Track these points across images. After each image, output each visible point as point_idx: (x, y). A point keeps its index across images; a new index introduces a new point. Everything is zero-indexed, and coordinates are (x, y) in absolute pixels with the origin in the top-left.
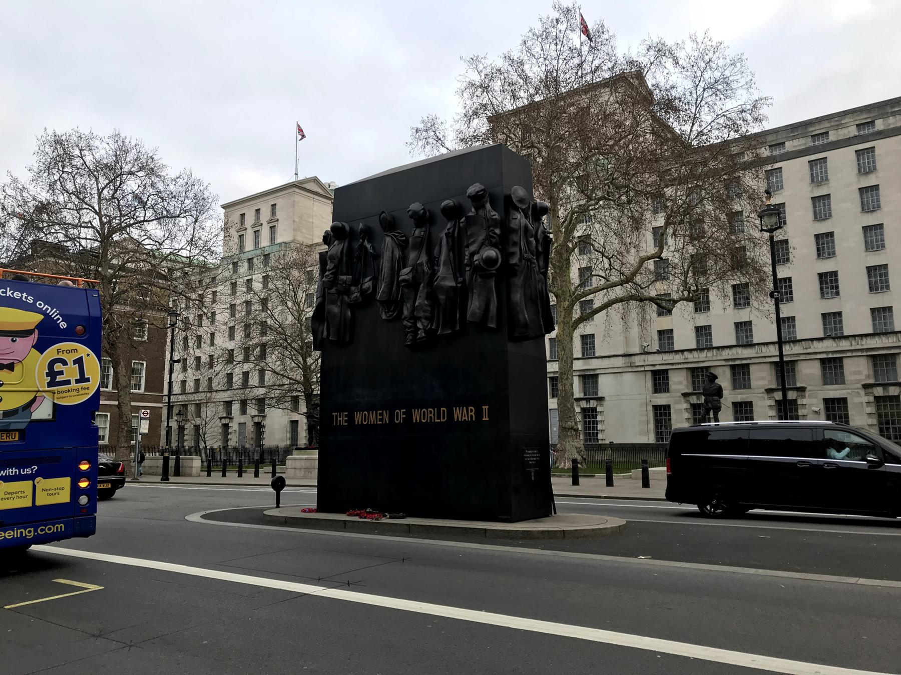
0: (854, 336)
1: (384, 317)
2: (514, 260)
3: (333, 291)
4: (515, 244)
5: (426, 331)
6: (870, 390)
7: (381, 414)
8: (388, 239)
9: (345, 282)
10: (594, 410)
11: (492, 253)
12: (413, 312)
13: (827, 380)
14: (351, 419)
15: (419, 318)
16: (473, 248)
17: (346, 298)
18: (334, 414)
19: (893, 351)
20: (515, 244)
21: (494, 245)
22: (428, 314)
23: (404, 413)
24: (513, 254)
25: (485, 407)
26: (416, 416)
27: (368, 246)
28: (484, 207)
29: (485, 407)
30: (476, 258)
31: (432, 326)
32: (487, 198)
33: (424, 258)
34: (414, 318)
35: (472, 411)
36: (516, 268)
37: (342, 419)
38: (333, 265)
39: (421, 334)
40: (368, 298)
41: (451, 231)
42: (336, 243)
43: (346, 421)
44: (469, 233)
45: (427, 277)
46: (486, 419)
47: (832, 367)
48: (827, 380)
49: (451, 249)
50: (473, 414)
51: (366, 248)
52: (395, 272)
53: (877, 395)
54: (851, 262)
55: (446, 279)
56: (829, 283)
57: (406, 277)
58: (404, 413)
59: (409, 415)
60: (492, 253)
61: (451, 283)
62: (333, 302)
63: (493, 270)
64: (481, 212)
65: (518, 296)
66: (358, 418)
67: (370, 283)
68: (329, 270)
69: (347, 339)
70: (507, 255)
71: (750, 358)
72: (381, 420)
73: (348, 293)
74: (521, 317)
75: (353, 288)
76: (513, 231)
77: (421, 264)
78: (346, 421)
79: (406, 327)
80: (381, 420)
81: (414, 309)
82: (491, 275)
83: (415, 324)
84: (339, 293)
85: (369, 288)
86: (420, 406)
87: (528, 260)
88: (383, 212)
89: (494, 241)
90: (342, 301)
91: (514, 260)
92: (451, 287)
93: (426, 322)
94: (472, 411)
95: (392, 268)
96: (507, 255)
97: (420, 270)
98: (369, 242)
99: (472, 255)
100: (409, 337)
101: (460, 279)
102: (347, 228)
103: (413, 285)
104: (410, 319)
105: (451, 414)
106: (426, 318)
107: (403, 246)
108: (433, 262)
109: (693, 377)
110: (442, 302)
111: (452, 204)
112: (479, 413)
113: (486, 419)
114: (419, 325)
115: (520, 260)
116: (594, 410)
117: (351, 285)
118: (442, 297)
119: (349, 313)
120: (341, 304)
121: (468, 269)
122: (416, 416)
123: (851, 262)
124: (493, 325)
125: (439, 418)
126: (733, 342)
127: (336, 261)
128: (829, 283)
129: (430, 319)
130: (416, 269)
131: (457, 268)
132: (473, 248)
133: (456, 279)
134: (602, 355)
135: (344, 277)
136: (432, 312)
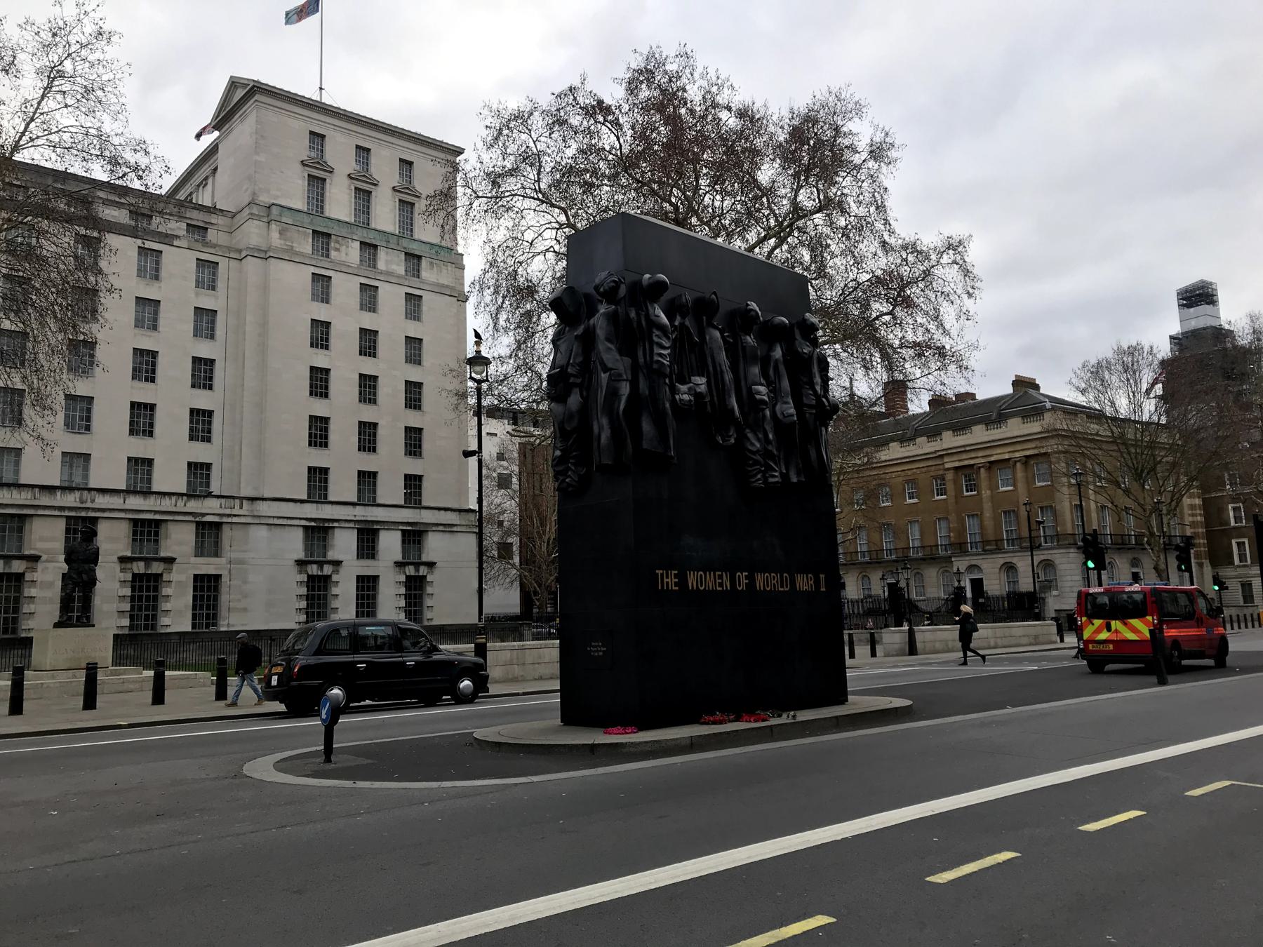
0: (33, 486)
6: (129, 566)
7: (721, 577)
10: (327, 578)
13: (200, 551)
18: (659, 572)
19: (157, 517)
26: (760, 580)
34: (767, 454)
46: (823, 589)
47: (368, 537)
48: (200, 551)
53: (136, 571)
54: (173, 395)
56: (142, 418)
59: (751, 579)
66: (692, 580)
71: (103, 510)
72: (721, 585)
79: (756, 462)
86: (763, 570)
105: (793, 582)
109: (135, 533)
116: (327, 578)
122: (760, 580)
123: (173, 395)
126: (122, 486)
128: (142, 418)
134: (433, 505)
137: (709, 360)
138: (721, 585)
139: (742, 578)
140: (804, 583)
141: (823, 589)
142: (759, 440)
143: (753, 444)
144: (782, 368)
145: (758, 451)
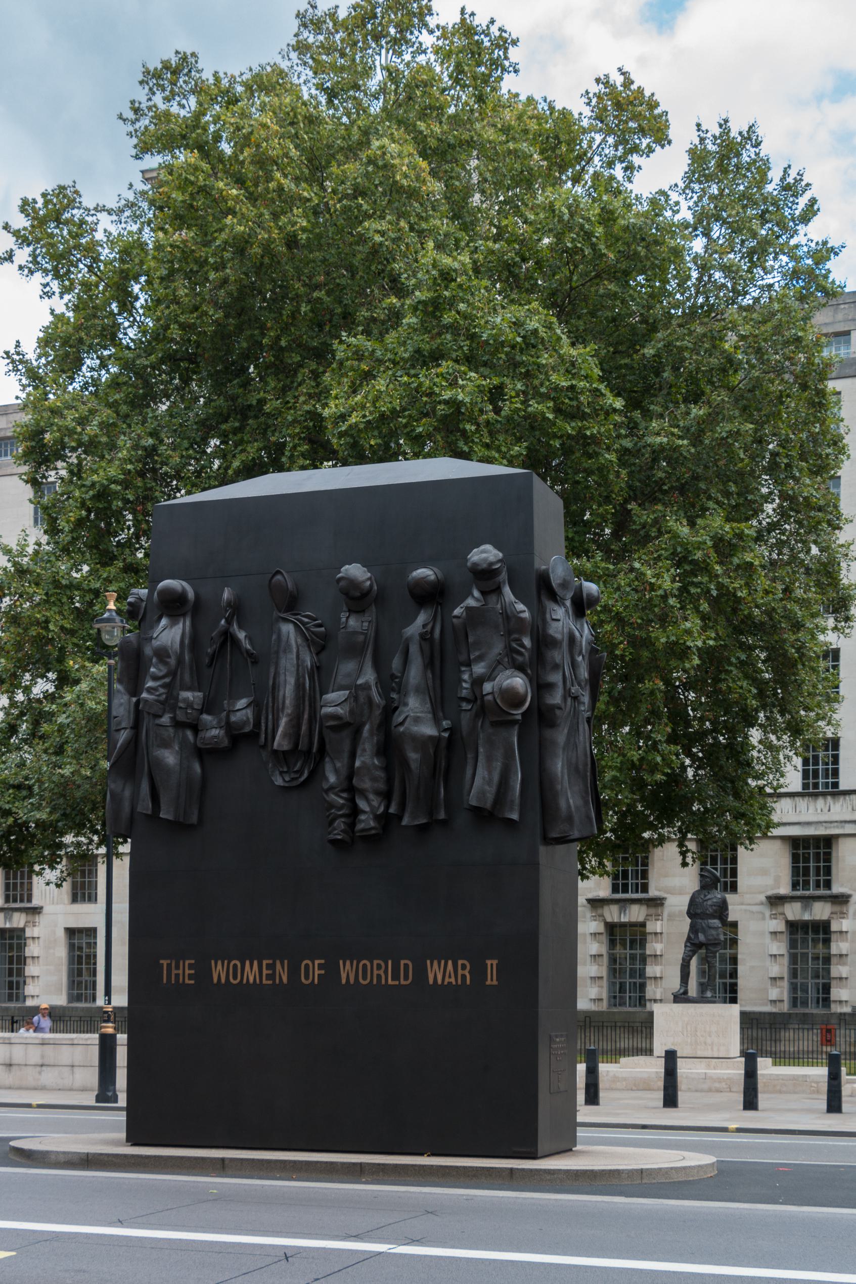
1: (279, 781)
2: (556, 698)
3: (166, 719)
4: (556, 667)
5: (377, 818)
7: (271, 967)
8: (288, 629)
9: (190, 705)
11: (518, 682)
12: (350, 777)
14: (203, 973)
15: (363, 793)
16: (479, 669)
17: (189, 734)
18: (165, 962)
20: (556, 667)
21: (521, 668)
22: (381, 786)
23: (321, 967)
24: (550, 686)
25: (492, 964)
26: (347, 971)
27: (241, 635)
28: (498, 590)
30: (487, 687)
31: (387, 807)
32: (504, 576)
33: (369, 676)
34: (351, 790)
35: (464, 967)
36: (558, 712)
38: (164, 670)
39: (366, 822)
40: (240, 738)
41: (429, 627)
42: (164, 622)
43: (190, 977)
44: (471, 640)
45: (377, 712)
46: (492, 980)
49: (429, 664)
50: (466, 973)
51: (235, 641)
52: (308, 699)
55: (418, 719)
57: (340, 710)
58: (321, 967)
59: (331, 971)
60: (518, 682)
61: (429, 730)
62: (166, 744)
63: (518, 713)
64: (494, 604)
65: (559, 766)
66: (219, 971)
67: (249, 712)
68: (155, 678)
69: (194, 819)
70: (541, 687)
72: (271, 977)
73: (196, 728)
74: (563, 804)
75: (206, 717)
76: (554, 643)
77: (366, 687)
78: (190, 977)
79: (331, 806)
80: (269, 977)
81: (351, 773)
82: (514, 722)
83: (352, 801)
84: (178, 725)
85: (246, 723)
86: (354, 955)
87: (575, 698)
88: (278, 572)
89: (520, 658)
90: (183, 743)
91: (556, 698)
92: (431, 738)
93: (375, 801)
94: (464, 967)
95: (299, 686)
96: (541, 687)
97: (362, 698)
98: (240, 627)
99: (478, 682)
100: (340, 824)
101: (446, 724)
102: (191, 594)
103: (350, 727)
104: (343, 791)
105: (421, 973)
106: (378, 793)
107: (320, 643)
108: (391, 684)
110: (414, 766)
111: (433, 577)
112: (479, 972)
113: (492, 980)
114: (362, 804)
115: (564, 699)
117: (201, 712)
118: (413, 756)
119: (197, 768)
120: (180, 748)
121: (465, 706)
122: (347, 971)
124: (515, 816)
127: (172, 661)
129: (387, 796)
130: (357, 691)
131: (441, 701)
132: (479, 669)
133: (437, 721)
135: (188, 695)
136: (389, 781)
137: (272, 670)
139: (314, 970)
140: (438, 973)
142: (336, 771)
143: (327, 779)
144: (414, 649)
145: (331, 788)
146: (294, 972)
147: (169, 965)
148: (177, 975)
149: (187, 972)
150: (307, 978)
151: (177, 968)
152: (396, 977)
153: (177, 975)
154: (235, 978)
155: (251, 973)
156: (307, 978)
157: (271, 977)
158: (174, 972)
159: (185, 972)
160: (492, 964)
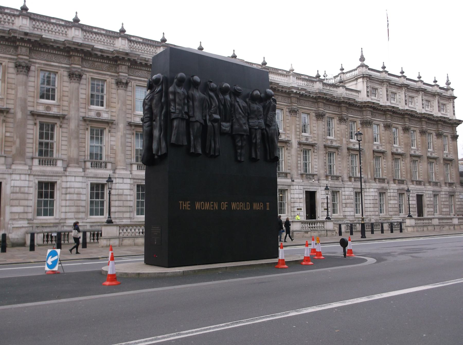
7: (213, 204)
14: (193, 205)
18: (181, 202)
23: (227, 204)
26: (234, 206)
29: (268, 203)
37: (186, 206)
46: (268, 209)
58: (227, 204)
59: (229, 205)
66: (198, 206)
72: (212, 207)
86: (235, 201)
105: (252, 207)
112: (265, 206)
125: (246, 208)
138: (213, 207)
139: (224, 206)
140: (256, 206)
141: (268, 209)
146: (219, 206)
147: (182, 203)
148: (185, 207)
149: (188, 206)
150: (223, 208)
151: (185, 204)
152: (246, 208)
153: (185, 207)
154: (203, 208)
155: (207, 206)
156: (223, 208)
157: (212, 207)
158: (184, 205)
159: (186, 206)
160: (268, 203)
